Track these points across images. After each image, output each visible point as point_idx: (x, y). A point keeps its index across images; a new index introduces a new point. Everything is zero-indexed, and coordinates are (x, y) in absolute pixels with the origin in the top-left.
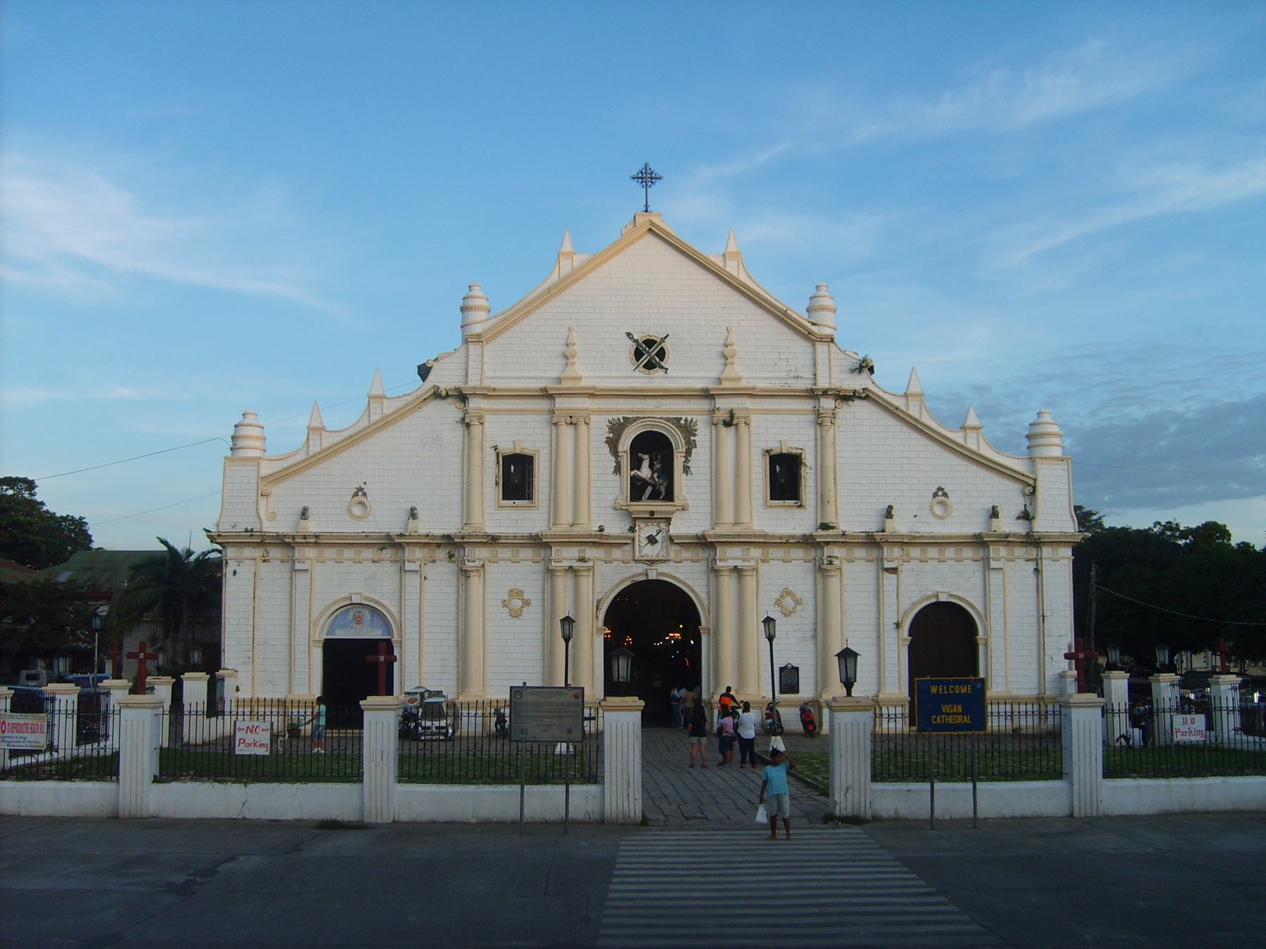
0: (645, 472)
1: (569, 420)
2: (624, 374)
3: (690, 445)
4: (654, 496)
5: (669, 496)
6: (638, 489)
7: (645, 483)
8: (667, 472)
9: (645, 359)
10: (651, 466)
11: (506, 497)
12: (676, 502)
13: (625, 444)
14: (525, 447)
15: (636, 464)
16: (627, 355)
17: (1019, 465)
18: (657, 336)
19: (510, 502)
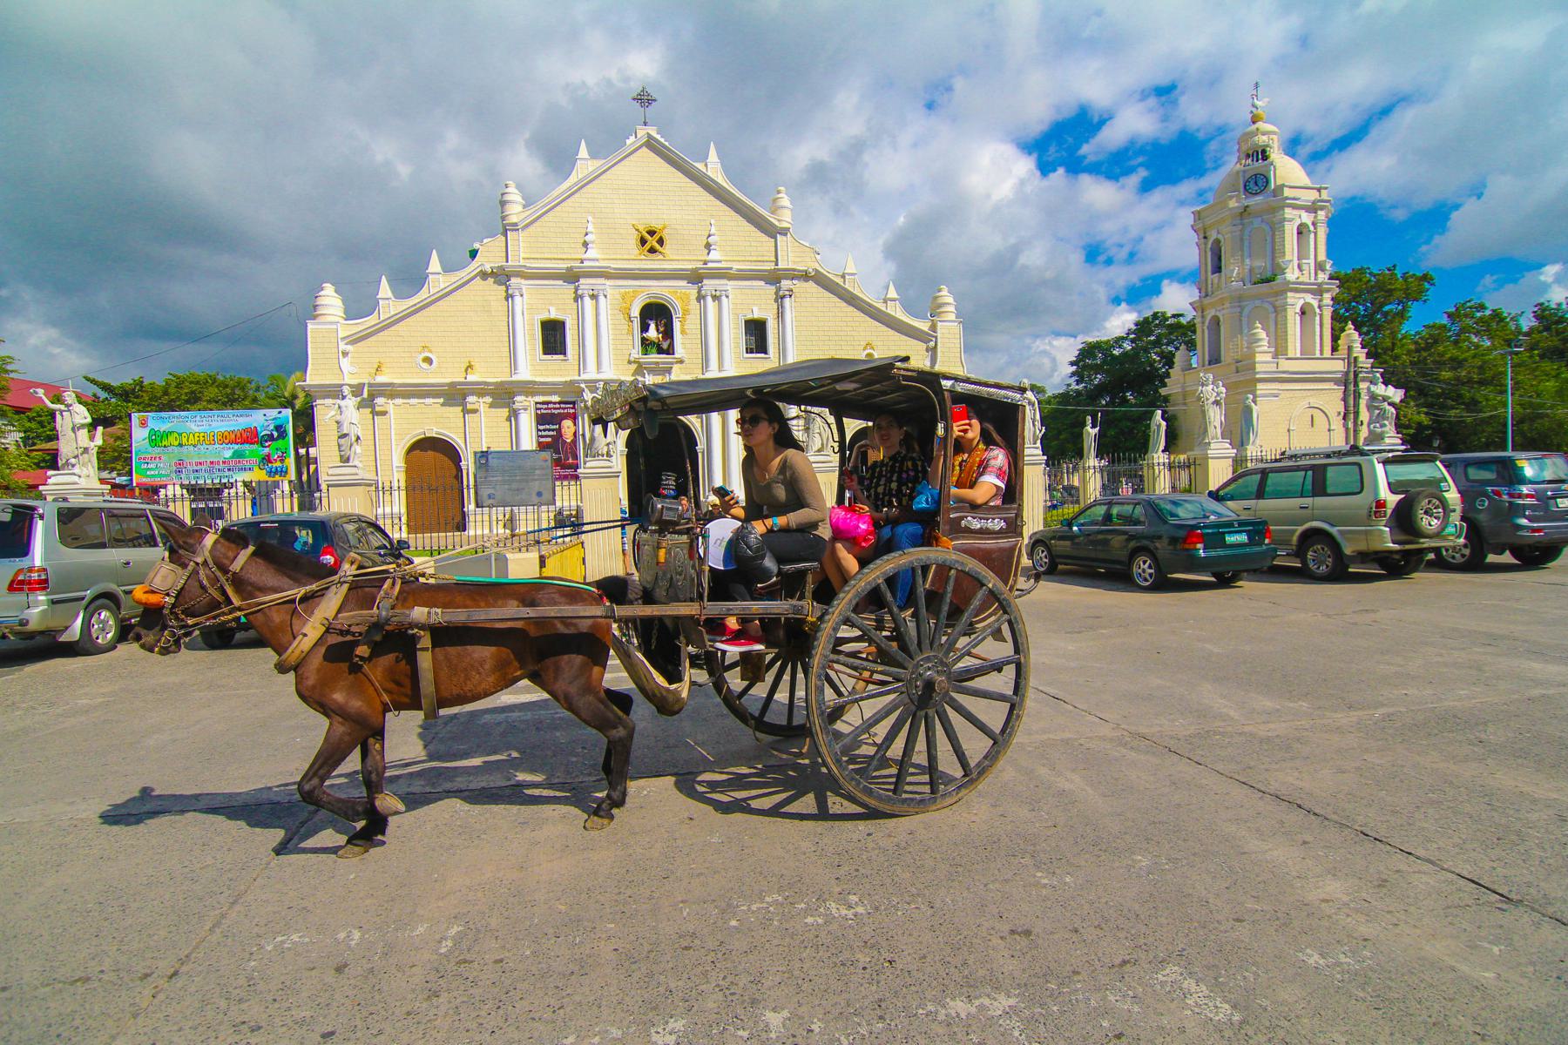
0: (652, 333)
1: (591, 293)
2: (633, 257)
3: (686, 312)
4: (660, 351)
5: (670, 351)
6: (646, 344)
7: (652, 343)
8: (668, 333)
9: (648, 246)
10: (658, 330)
11: (545, 353)
12: (676, 356)
13: (636, 312)
14: (560, 317)
15: (645, 328)
16: (634, 242)
17: (924, 326)
18: (655, 225)
19: (549, 357)
